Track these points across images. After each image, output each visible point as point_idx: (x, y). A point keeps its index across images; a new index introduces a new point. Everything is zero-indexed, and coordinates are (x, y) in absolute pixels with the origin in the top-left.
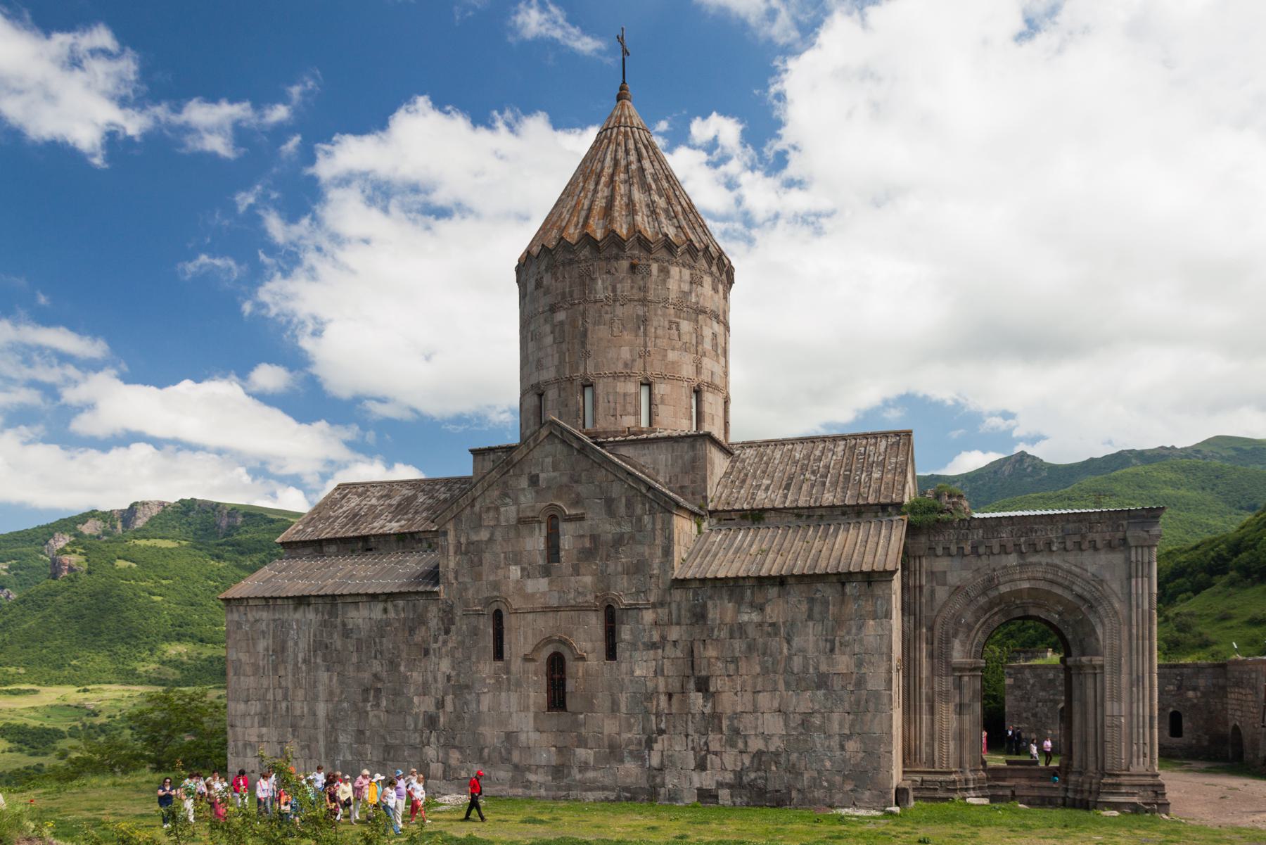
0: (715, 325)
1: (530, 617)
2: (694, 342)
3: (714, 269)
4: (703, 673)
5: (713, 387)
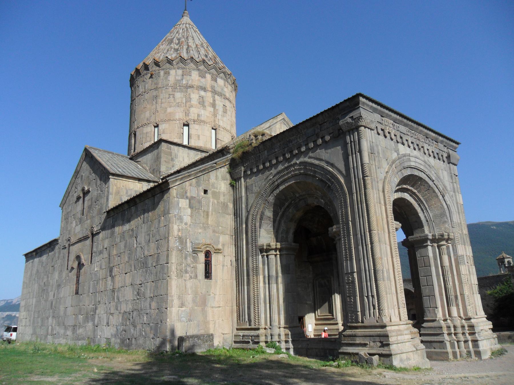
0: (202, 93)
1: (76, 245)
2: (184, 101)
3: (202, 67)
4: (112, 265)
5: (199, 121)
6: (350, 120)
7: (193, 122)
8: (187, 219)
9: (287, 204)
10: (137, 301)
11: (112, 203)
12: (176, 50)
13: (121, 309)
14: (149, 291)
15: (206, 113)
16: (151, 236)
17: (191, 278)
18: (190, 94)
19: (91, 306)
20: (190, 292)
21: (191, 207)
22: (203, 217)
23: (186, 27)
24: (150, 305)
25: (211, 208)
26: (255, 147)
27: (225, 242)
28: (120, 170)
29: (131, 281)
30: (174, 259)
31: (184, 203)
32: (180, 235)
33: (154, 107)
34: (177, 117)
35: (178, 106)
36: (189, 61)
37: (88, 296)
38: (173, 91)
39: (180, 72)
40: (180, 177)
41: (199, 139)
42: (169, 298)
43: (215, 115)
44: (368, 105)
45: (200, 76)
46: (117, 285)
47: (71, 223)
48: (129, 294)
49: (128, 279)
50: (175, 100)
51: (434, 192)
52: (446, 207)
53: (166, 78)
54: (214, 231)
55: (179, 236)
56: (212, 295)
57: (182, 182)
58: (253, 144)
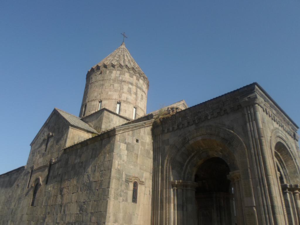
0: (130, 86)
2: (119, 89)
3: (132, 72)
5: (127, 102)
6: (247, 100)
7: (123, 102)
8: (125, 158)
9: (193, 154)
10: (80, 215)
11: (69, 144)
12: (118, 61)
13: (65, 220)
14: (90, 208)
15: (132, 98)
16: (97, 167)
17: (123, 200)
18: (123, 86)
19: (42, 215)
20: (122, 211)
21: (127, 149)
22: (135, 158)
23: (123, 50)
24: (91, 219)
25: (139, 153)
26: (172, 115)
27: (147, 177)
28: (76, 124)
29: (76, 198)
30: (114, 184)
31: (123, 146)
32: (119, 168)
33: (101, 90)
34: (114, 98)
35: (115, 91)
36: (125, 67)
37: (41, 207)
38: (113, 82)
39: (118, 72)
40: (123, 128)
41: (126, 112)
42: (108, 215)
43: (136, 100)
44: (259, 91)
45: (130, 76)
46: (65, 202)
47: (36, 156)
48: (74, 209)
49: (74, 197)
50: (113, 88)
51: (290, 156)
52: (297, 167)
53: (110, 75)
54: (140, 169)
55: (118, 169)
56: (136, 215)
57: (123, 132)
58: (171, 113)
